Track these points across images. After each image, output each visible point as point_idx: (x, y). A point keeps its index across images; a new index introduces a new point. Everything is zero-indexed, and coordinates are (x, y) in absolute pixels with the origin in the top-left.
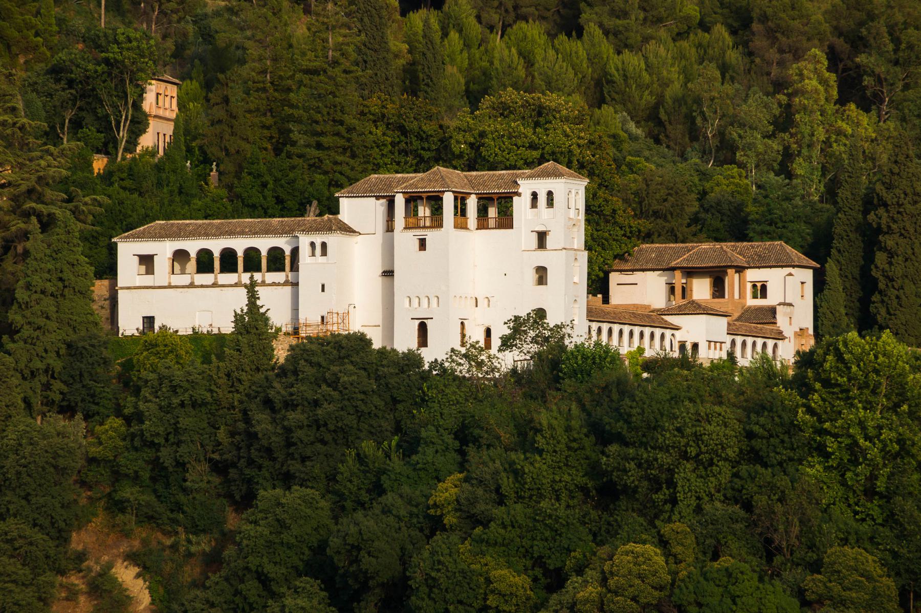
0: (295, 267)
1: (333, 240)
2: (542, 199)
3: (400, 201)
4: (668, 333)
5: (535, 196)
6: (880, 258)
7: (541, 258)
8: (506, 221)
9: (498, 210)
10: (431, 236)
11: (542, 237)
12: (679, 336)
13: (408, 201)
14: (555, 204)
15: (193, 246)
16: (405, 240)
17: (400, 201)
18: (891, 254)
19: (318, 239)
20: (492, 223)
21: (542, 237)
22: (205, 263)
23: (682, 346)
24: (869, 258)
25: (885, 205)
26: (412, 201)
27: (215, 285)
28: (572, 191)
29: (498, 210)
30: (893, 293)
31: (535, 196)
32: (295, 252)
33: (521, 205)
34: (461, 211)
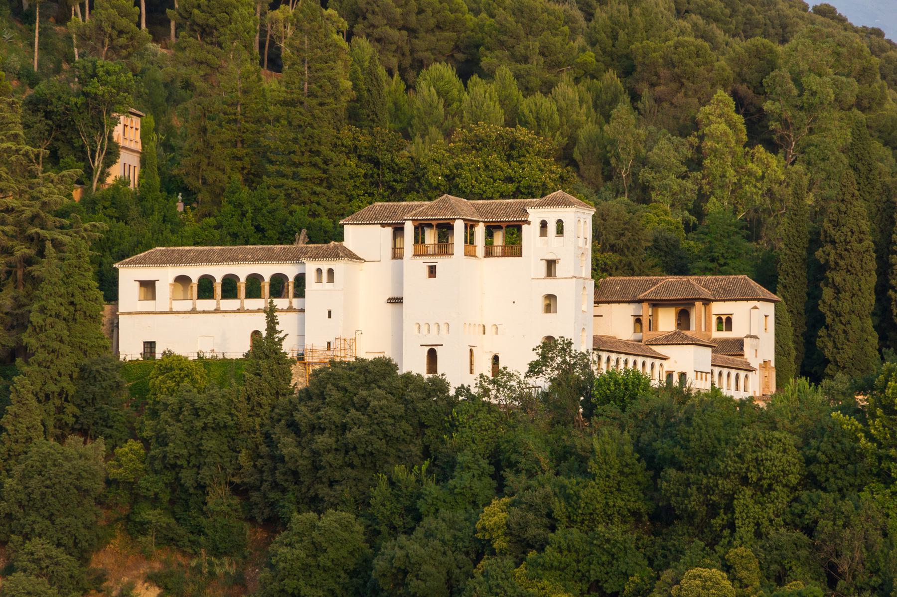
0: (300, 292)
1: (340, 266)
2: (552, 228)
3: (409, 227)
4: (657, 362)
5: (544, 225)
6: (827, 293)
7: (550, 285)
8: (514, 248)
9: (509, 237)
10: (441, 262)
11: (551, 265)
12: (668, 366)
13: (416, 228)
14: (563, 232)
15: (195, 272)
16: (414, 267)
17: (409, 227)
18: (838, 291)
19: (325, 265)
20: (498, 250)
21: (551, 265)
22: (206, 288)
23: (670, 375)
24: (814, 296)
25: (833, 242)
26: (420, 228)
27: (217, 311)
28: (579, 220)
29: (509, 237)
30: (839, 328)
31: (544, 225)
32: (300, 280)
33: (530, 233)
34: (470, 240)
